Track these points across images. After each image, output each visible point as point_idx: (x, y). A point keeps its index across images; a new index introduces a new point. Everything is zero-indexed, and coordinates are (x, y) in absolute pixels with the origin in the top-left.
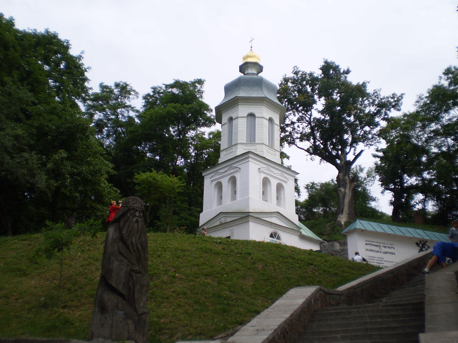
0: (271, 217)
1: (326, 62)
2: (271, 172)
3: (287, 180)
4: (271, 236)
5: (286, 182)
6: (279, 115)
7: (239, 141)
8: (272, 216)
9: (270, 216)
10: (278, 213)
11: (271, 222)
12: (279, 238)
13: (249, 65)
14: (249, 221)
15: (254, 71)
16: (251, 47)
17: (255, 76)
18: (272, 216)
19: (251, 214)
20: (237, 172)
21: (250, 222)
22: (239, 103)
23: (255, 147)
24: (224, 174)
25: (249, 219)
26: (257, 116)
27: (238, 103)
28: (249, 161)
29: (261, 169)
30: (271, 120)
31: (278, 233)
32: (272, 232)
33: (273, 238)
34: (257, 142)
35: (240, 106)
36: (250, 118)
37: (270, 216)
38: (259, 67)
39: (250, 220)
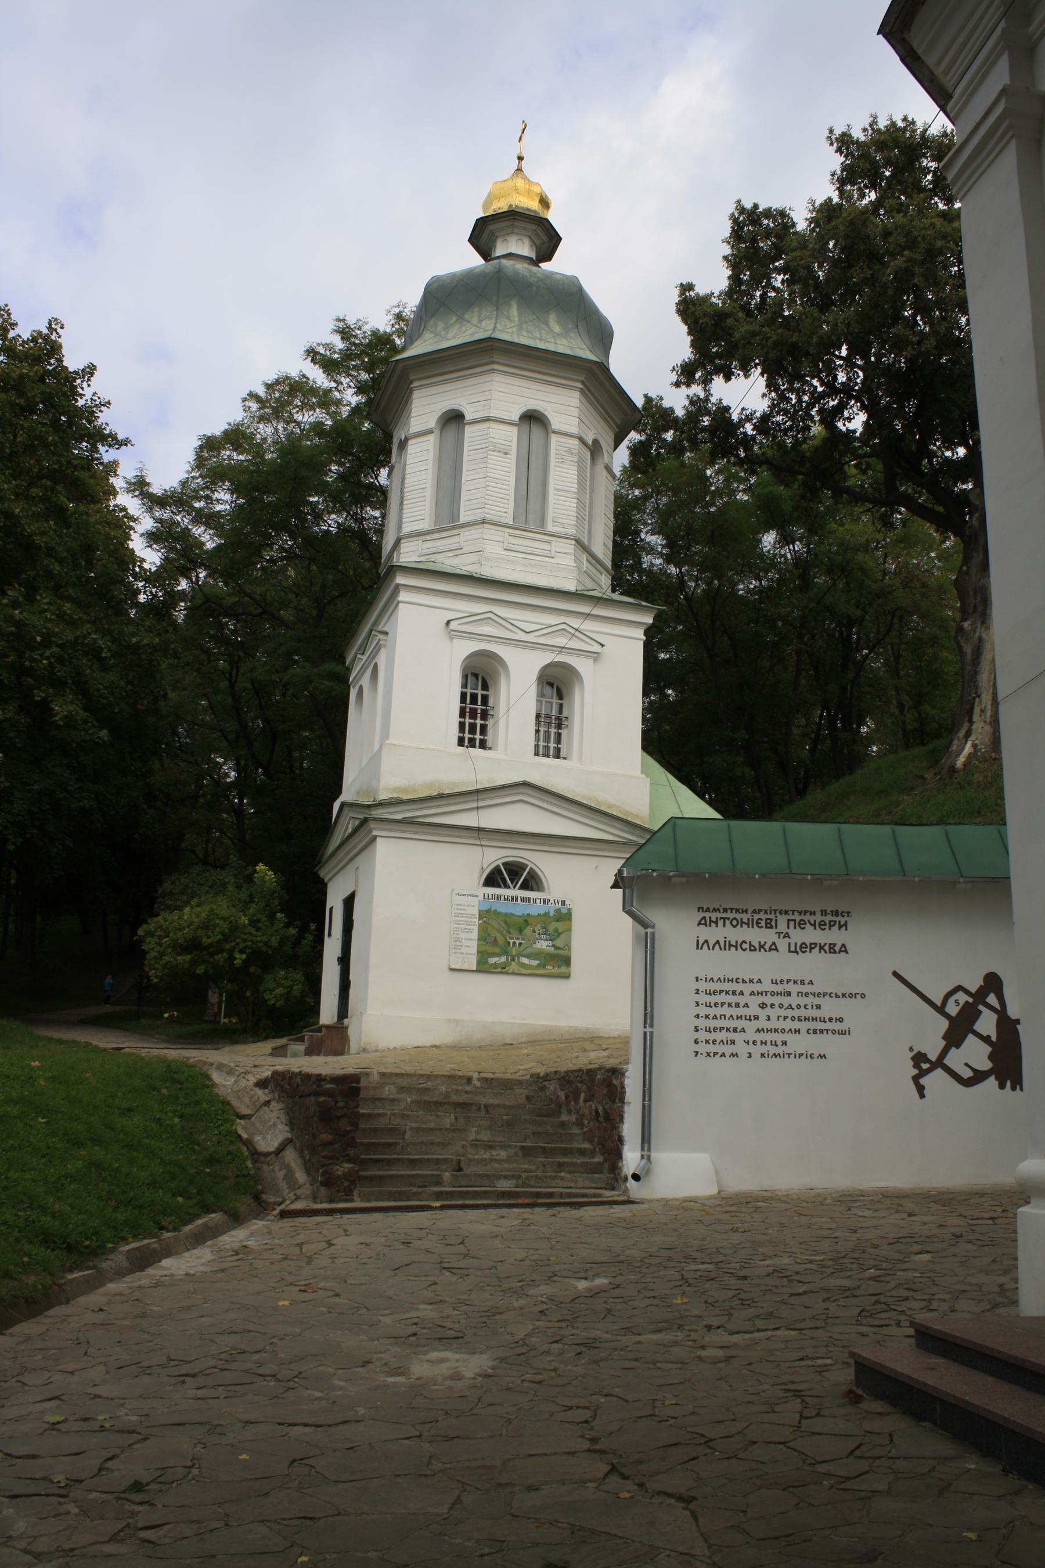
0: (478, 808)
1: (844, 142)
2: (510, 630)
3: (596, 648)
4: (493, 879)
5: (596, 656)
6: (577, 394)
7: (407, 528)
8: (481, 804)
9: (475, 805)
10: (525, 784)
11: (479, 830)
12: (532, 882)
13: (492, 227)
14: (374, 839)
15: (525, 249)
16: (520, 158)
17: (521, 267)
18: (481, 804)
19: (377, 813)
20: (380, 648)
21: (378, 839)
22: (415, 384)
23: (455, 539)
24: (365, 658)
25: (371, 831)
26: (468, 417)
27: (411, 383)
28: (399, 602)
29: (453, 625)
30: (533, 419)
31: (530, 865)
32: (500, 863)
33: (507, 886)
34: (463, 520)
35: (416, 394)
36: (451, 430)
37: (475, 805)
38: (534, 227)
39: (375, 833)
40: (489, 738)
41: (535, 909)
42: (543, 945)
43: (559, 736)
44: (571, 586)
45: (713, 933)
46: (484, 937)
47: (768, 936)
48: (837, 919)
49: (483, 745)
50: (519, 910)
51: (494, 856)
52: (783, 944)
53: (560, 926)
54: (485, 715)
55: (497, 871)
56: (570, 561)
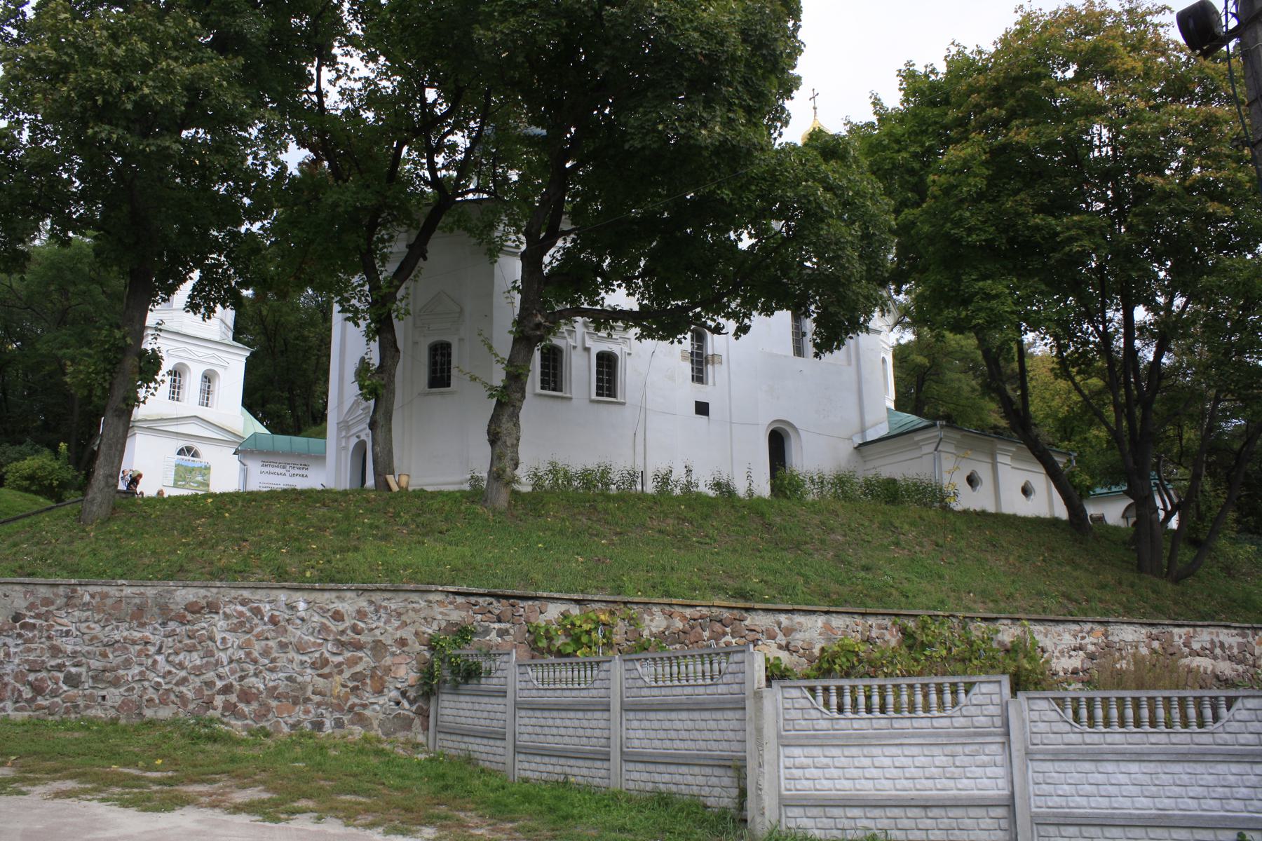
4: (181, 452)
5: (225, 368)
10: (196, 417)
12: (196, 454)
34: (174, 307)
40: (180, 397)
41: (196, 465)
42: (199, 479)
43: (208, 399)
44: (217, 338)
45: (266, 469)
46: (176, 473)
47: (283, 471)
48: (305, 467)
49: (178, 400)
50: (190, 465)
51: (182, 443)
52: (287, 474)
53: (206, 472)
54: (179, 388)
55: (182, 449)
56: (217, 328)
